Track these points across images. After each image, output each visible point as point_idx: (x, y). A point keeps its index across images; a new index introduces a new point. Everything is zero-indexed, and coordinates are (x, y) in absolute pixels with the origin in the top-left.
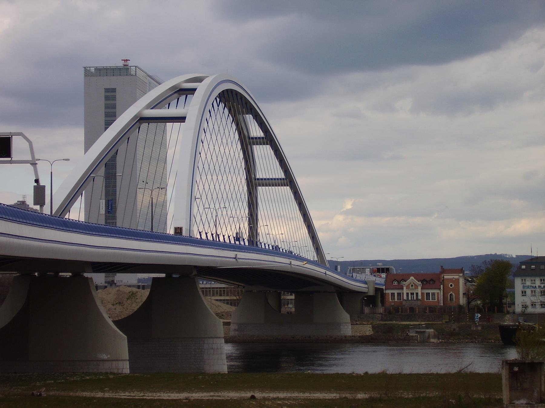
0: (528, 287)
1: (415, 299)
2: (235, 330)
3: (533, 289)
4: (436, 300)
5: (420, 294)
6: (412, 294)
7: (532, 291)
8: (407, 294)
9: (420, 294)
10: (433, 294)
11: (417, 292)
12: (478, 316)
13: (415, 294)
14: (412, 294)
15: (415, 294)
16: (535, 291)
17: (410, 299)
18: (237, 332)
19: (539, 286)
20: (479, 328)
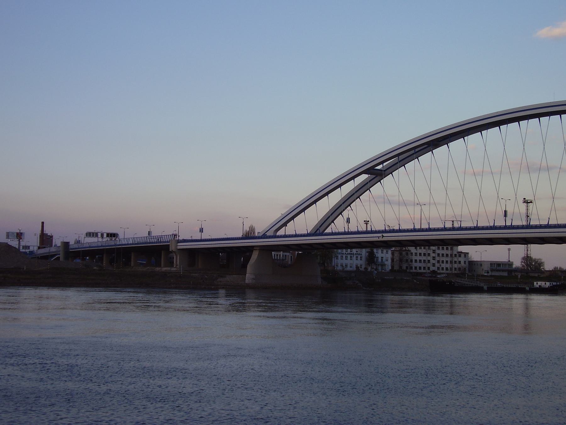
0: (340, 254)
1: (279, 258)
2: (253, 279)
3: (342, 255)
4: (287, 260)
5: (281, 256)
6: (277, 255)
7: (341, 256)
8: (275, 255)
9: (281, 256)
10: (286, 255)
11: (280, 254)
12: (375, 273)
13: (279, 255)
14: (277, 255)
15: (279, 255)
16: (342, 256)
17: (276, 258)
18: (254, 281)
19: (345, 253)
20: (380, 281)
